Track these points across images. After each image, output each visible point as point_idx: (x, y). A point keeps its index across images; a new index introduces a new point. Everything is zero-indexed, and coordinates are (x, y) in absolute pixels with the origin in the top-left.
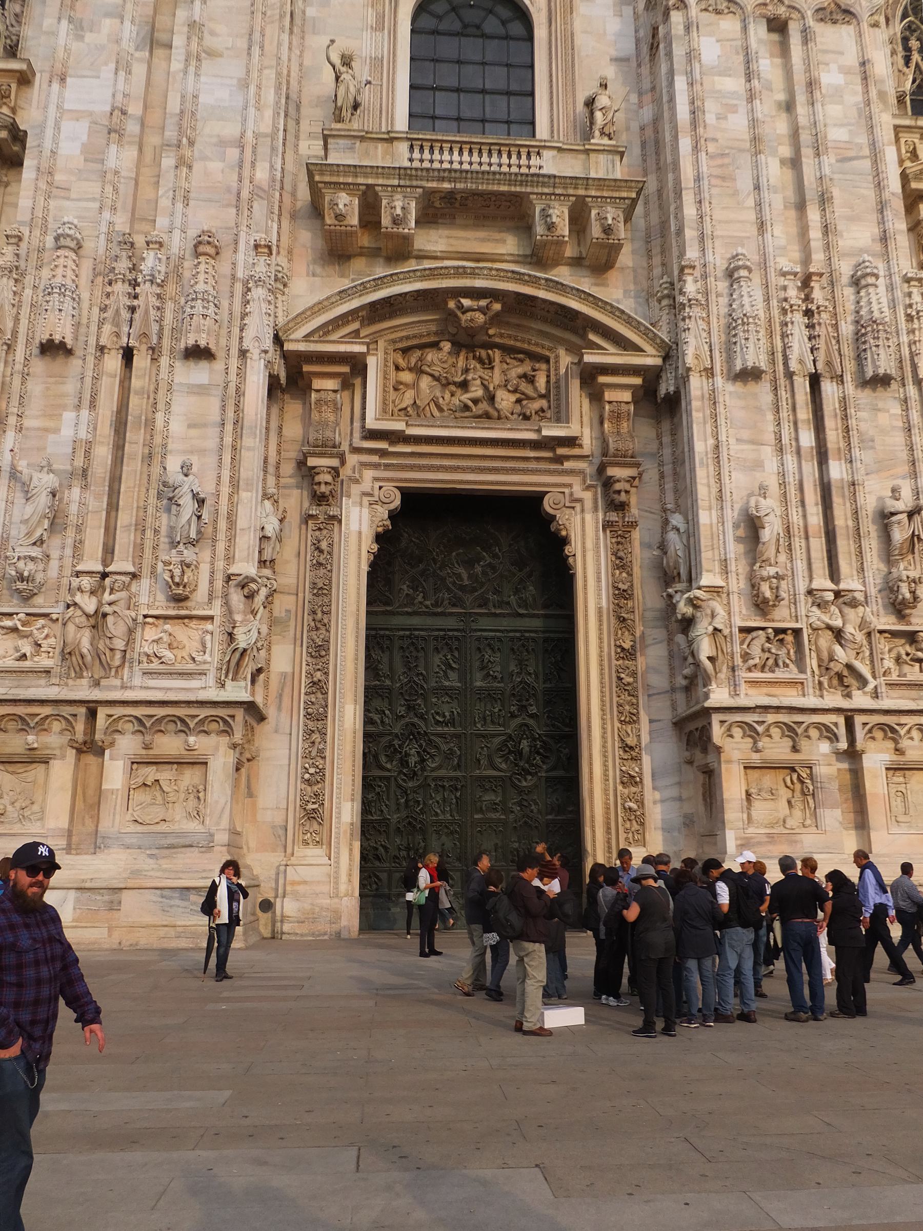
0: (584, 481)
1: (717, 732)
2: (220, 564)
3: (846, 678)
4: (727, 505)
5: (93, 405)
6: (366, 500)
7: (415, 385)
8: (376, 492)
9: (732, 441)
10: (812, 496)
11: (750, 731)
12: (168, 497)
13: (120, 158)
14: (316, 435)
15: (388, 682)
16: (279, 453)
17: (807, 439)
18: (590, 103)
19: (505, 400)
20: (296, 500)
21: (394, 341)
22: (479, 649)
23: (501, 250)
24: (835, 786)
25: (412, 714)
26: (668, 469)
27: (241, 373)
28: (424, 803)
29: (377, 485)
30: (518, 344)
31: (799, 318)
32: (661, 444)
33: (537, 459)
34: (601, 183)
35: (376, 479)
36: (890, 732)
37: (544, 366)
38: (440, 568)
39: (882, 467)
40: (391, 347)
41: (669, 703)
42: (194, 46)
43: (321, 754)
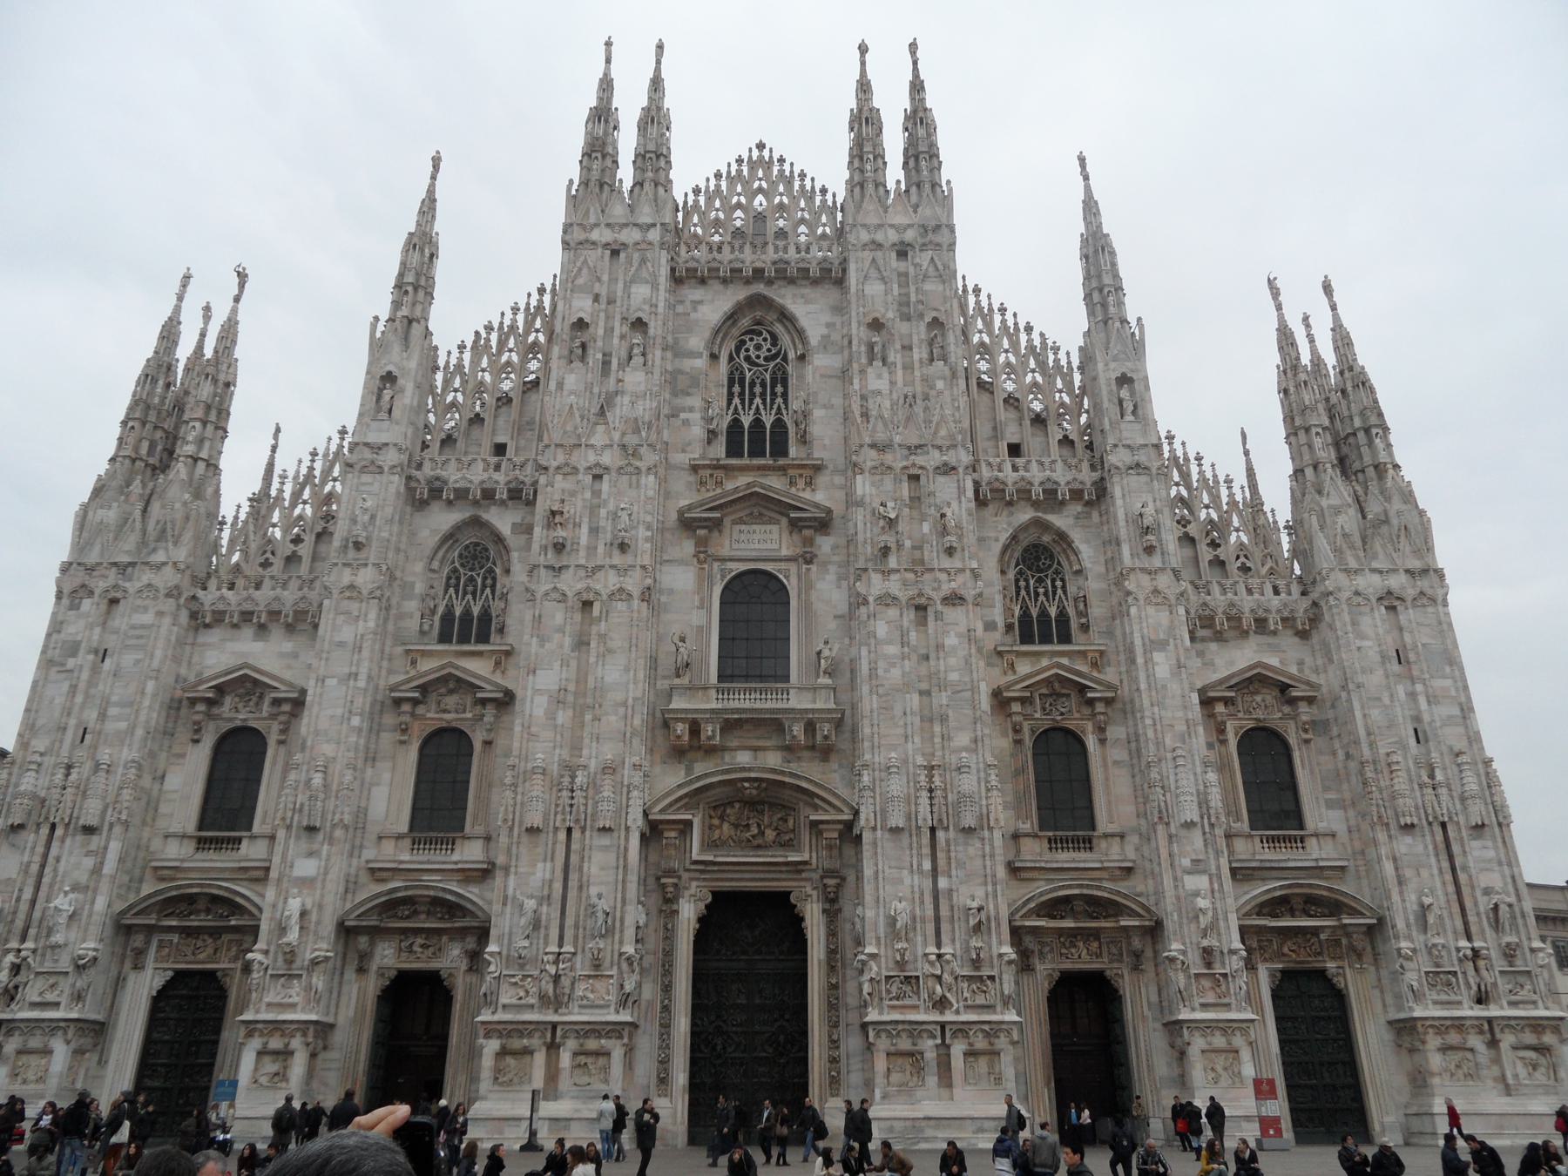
1: (871, 1034)
2: (616, 947)
3: (941, 1004)
5: (552, 860)
7: (720, 827)
10: (928, 899)
11: (889, 1035)
12: (591, 910)
13: (563, 717)
17: (927, 865)
18: (819, 653)
19: (770, 835)
20: (654, 900)
23: (768, 743)
24: (934, 1064)
27: (627, 839)
31: (925, 794)
34: (821, 711)
42: (602, 649)
43: (668, 1046)
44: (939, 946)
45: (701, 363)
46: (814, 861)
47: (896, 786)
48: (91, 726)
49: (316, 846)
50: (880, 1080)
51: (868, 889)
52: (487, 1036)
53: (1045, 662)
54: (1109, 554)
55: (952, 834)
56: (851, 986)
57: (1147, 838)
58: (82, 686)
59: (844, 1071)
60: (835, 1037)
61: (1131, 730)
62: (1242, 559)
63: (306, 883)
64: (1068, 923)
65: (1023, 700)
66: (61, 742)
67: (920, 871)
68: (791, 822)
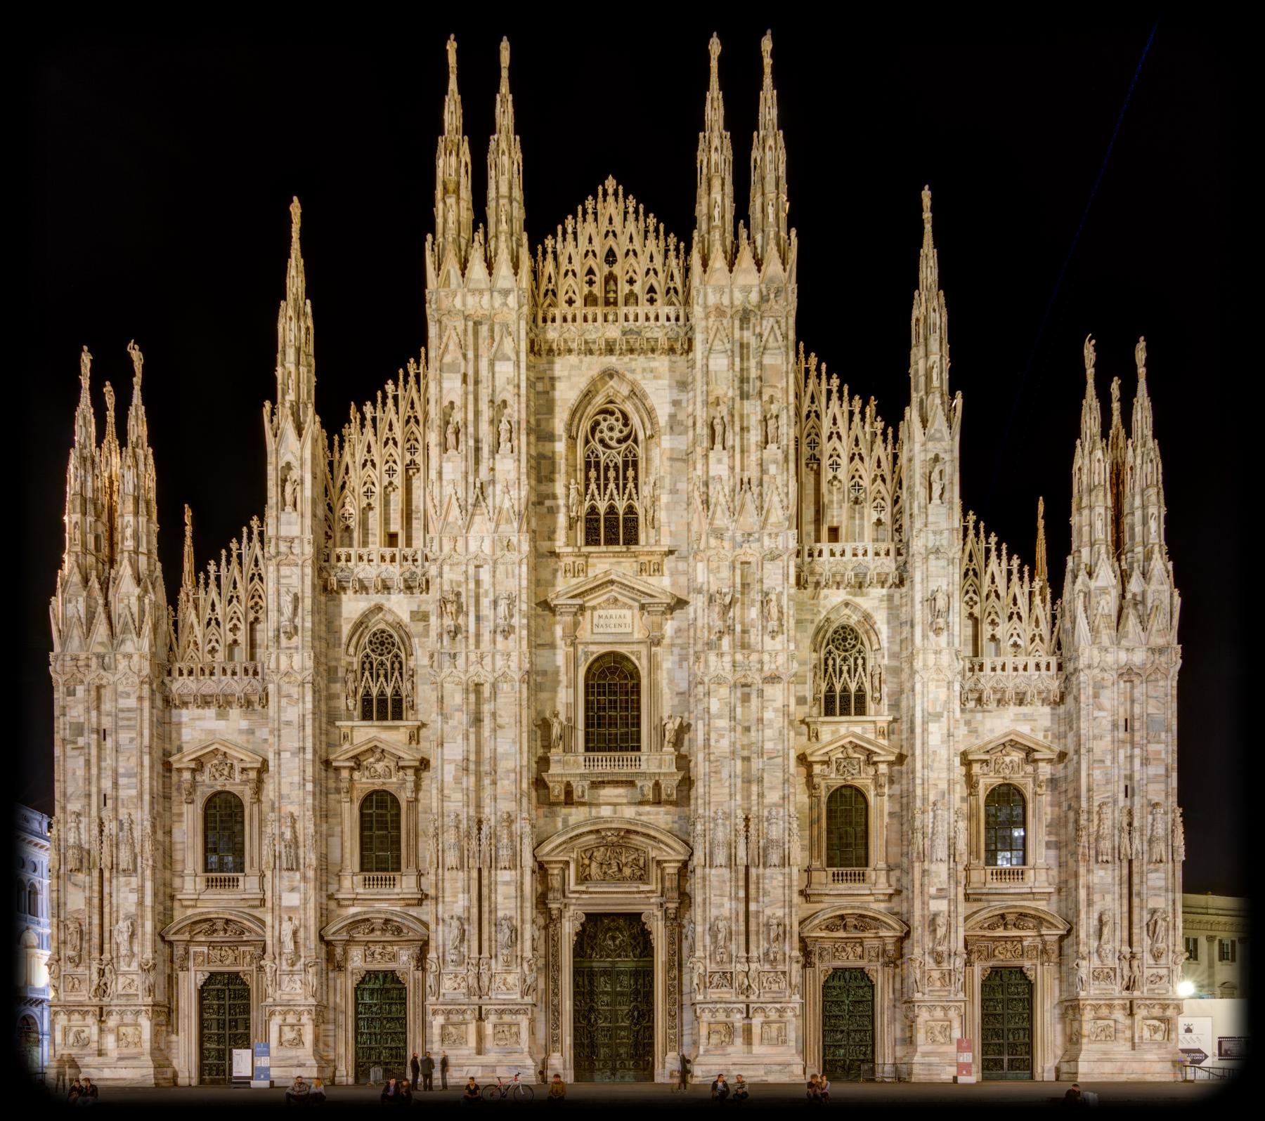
11: (710, 1010)
17: (742, 894)
27: (522, 875)
36: (763, 1010)
39: (771, 904)
44: (747, 951)
45: (560, 447)
47: (720, 835)
48: (109, 792)
49: (296, 884)
50: (703, 1040)
51: (699, 911)
52: (435, 1013)
53: (843, 730)
54: (904, 635)
55: (761, 870)
56: (686, 978)
57: (907, 871)
58: (94, 760)
61: (905, 787)
62: (1015, 638)
63: (292, 909)
64: (841, 934)
65: (824, 763)
66: (89, 805)
67: (737, 899)
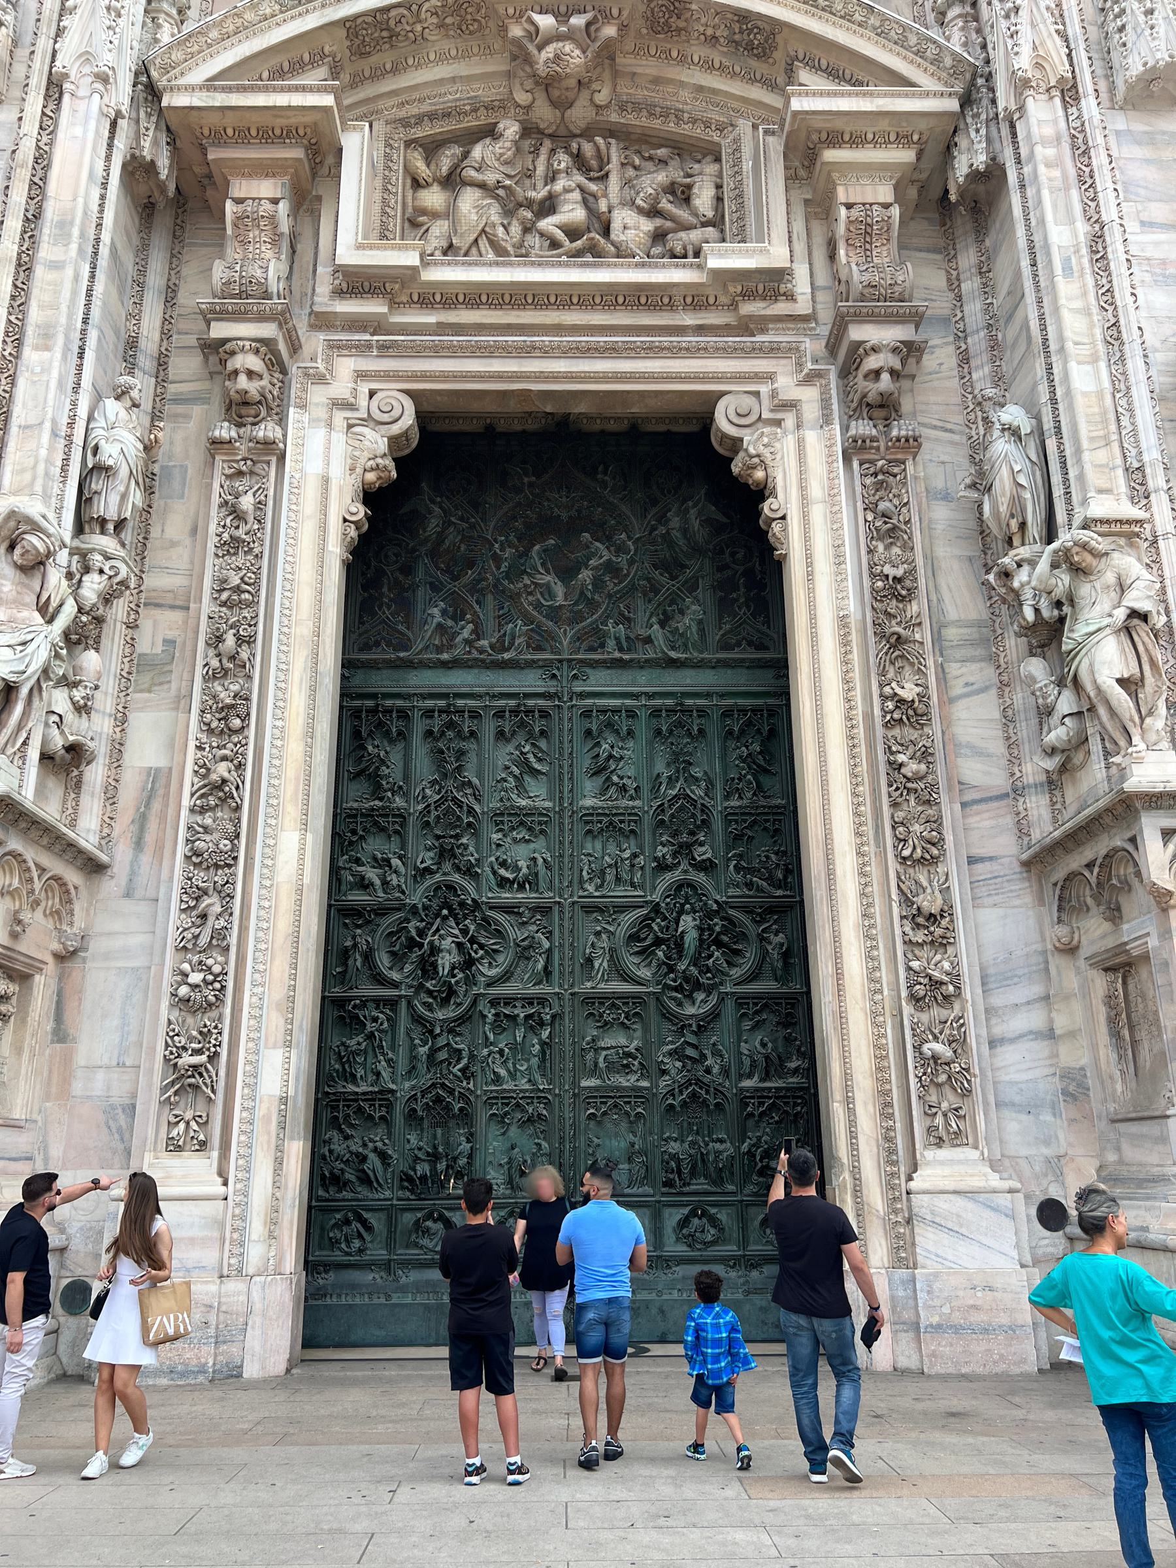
0: (800, 365)
4: (1133, 352)
6: (340, 417)
7: (450, 213)
8: (363, 402)
9: (1132, 226)
14: (228, 274)
15: (399, 802)
16: (166, 335)
21: (405, 123)
22: (588, 733)
25: (447, 866)
26: (977, 342)
28: (472, 1057)
29: (364, 388)
30: (657, 123)
32: (959, 298)
33: (700, 329)
35: (361, 375)
37: (711, 168)
38: (507, 576)
40: (402, 134)
41: (1009, 821)
46: (801, 285)
59: (975, 1034)
60: (930, 902)
68: (703, 199)
